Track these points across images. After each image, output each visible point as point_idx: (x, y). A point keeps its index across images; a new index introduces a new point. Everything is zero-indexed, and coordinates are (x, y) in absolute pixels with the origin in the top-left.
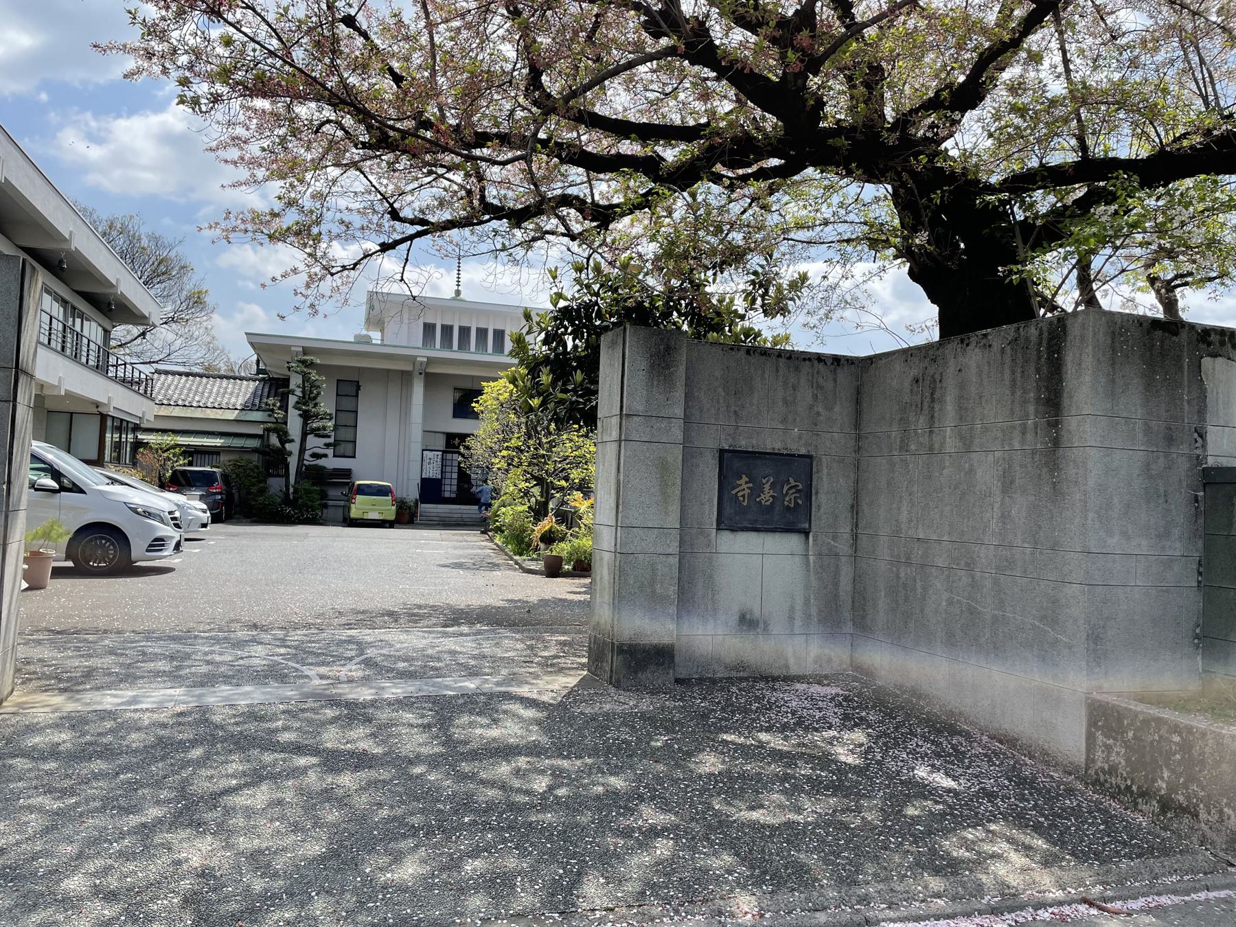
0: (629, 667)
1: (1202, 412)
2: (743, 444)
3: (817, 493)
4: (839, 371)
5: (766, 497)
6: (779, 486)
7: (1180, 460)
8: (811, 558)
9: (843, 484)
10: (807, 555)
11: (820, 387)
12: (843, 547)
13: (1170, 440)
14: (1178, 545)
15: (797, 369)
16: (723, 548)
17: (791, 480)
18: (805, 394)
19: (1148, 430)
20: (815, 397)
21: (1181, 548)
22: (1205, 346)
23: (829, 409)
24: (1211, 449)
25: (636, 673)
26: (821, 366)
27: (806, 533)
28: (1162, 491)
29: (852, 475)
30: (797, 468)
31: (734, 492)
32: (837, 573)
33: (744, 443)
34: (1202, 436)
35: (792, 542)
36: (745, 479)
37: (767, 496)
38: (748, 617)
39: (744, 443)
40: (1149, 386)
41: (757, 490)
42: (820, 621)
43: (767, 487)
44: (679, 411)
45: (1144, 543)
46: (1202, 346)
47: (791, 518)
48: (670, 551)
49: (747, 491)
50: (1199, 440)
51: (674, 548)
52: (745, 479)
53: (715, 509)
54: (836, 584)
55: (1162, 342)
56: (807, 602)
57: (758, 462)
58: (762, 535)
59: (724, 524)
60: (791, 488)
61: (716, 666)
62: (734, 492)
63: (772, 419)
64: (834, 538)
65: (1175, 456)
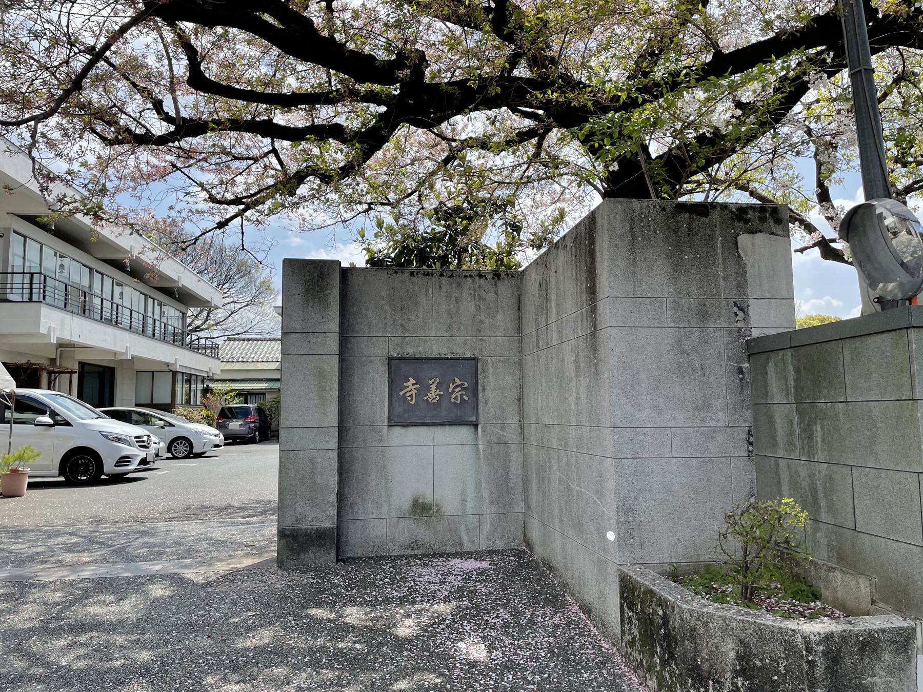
0: (292, 550)
1: (741, 287)
2: (411, 351)
3: (484, 390)
4: (500, 284)
5: (433, 394)
6: (444, 386)
7: (718, 334)
8: (481, 447)
9: (509, 380)
10: (476, 445)
11: (481, 299)
12: (512, 435)
13: (704, 314)
14: (721, 415)
15: (459, 285)
16: (395, 442)
17: (456, 379)
18: (468, 306)
19: (676, 307)
20: (478, 308)
21: (724, 417)
22: (742, 224)
23: (492, 316)
24: (754, 321)
25: (298, 554)
26: (482, 280)
27: (476, 426)
28: (698, 365)
29: (518, 373)
30: (468, 369)
31: (401, 393)
32: (507, 457)
33: (411, 351)
34: (743, 309)
35: (463, 433)
36: (412, 381)
37: (434, 395)
38: (421, 501)
39: (411, 351)
40: (677, 266)
41: (424, 389)
42: (491, 503)
43: (434, 387)
44: (334, 326)
45: (680, 416)
46: (736, 223)
47: (463, 415)
48: (330, 447)
49: (414, 392)
50: (740, 313)
51: (334, 443)
52: (412, 381)
53: (386, 409)
54: (507, 469)
55: (690, 224)
56: (478, 485)
57: (425, 366)
58: (432, 429)
59: (392, 422)
60: (457, 386)
61: (391, 545)
62: (401, 393)
63: (438, 329)
64: (503, 428)
65: (711, 330)
